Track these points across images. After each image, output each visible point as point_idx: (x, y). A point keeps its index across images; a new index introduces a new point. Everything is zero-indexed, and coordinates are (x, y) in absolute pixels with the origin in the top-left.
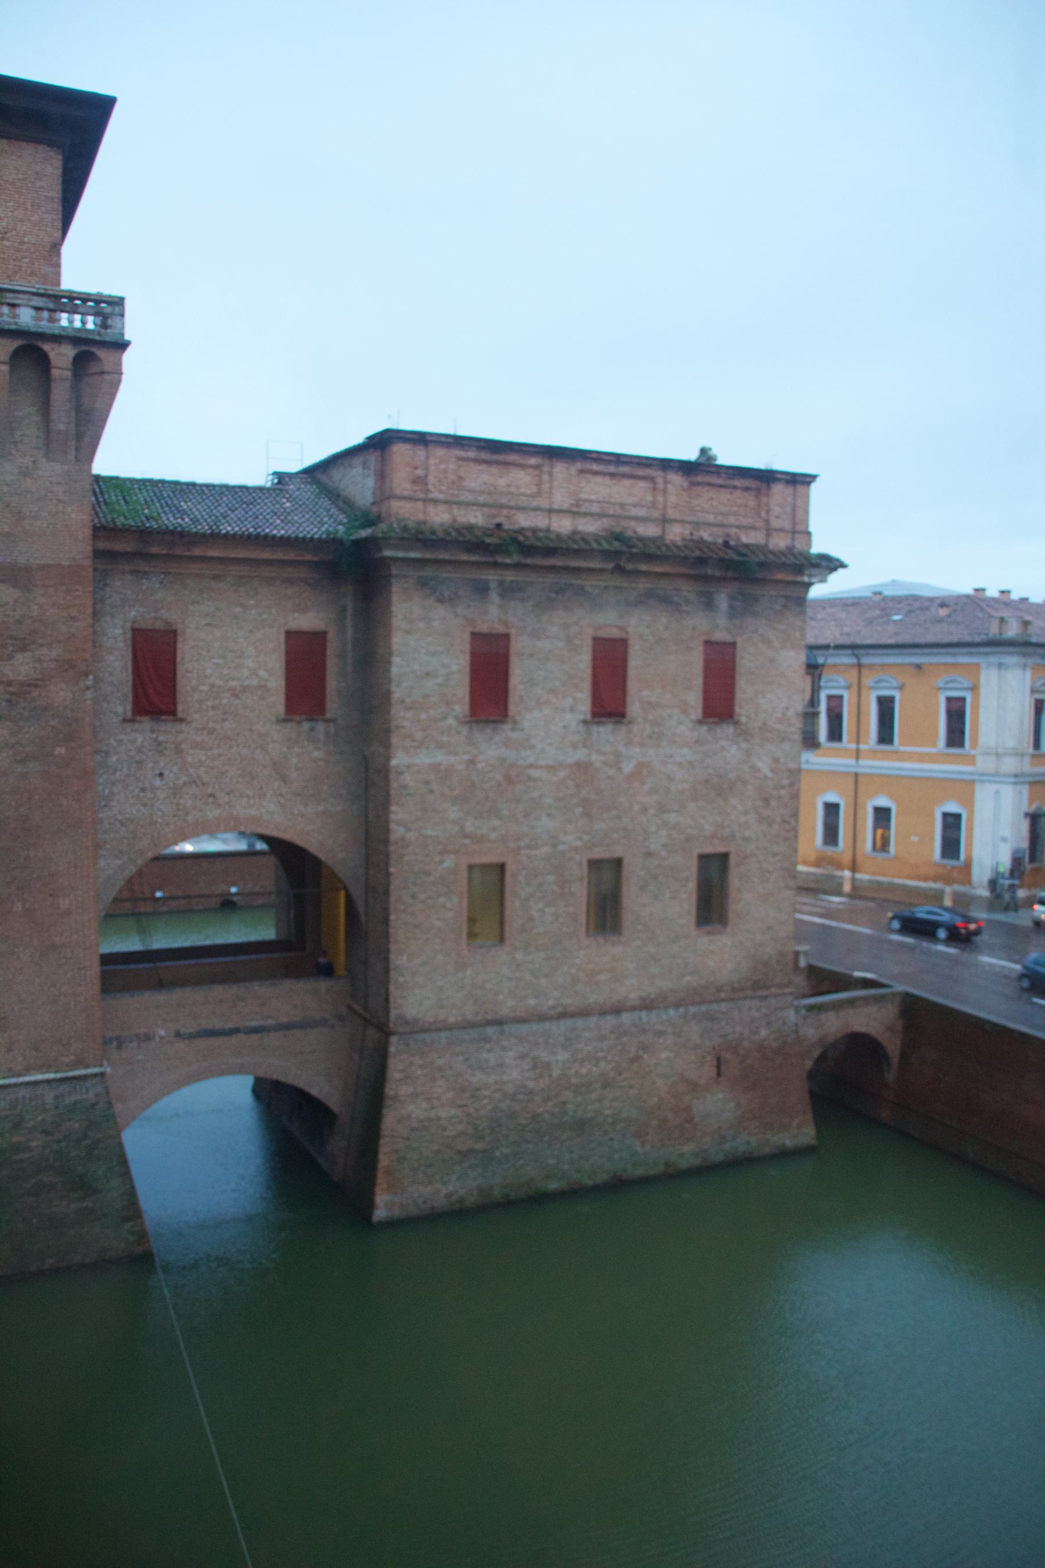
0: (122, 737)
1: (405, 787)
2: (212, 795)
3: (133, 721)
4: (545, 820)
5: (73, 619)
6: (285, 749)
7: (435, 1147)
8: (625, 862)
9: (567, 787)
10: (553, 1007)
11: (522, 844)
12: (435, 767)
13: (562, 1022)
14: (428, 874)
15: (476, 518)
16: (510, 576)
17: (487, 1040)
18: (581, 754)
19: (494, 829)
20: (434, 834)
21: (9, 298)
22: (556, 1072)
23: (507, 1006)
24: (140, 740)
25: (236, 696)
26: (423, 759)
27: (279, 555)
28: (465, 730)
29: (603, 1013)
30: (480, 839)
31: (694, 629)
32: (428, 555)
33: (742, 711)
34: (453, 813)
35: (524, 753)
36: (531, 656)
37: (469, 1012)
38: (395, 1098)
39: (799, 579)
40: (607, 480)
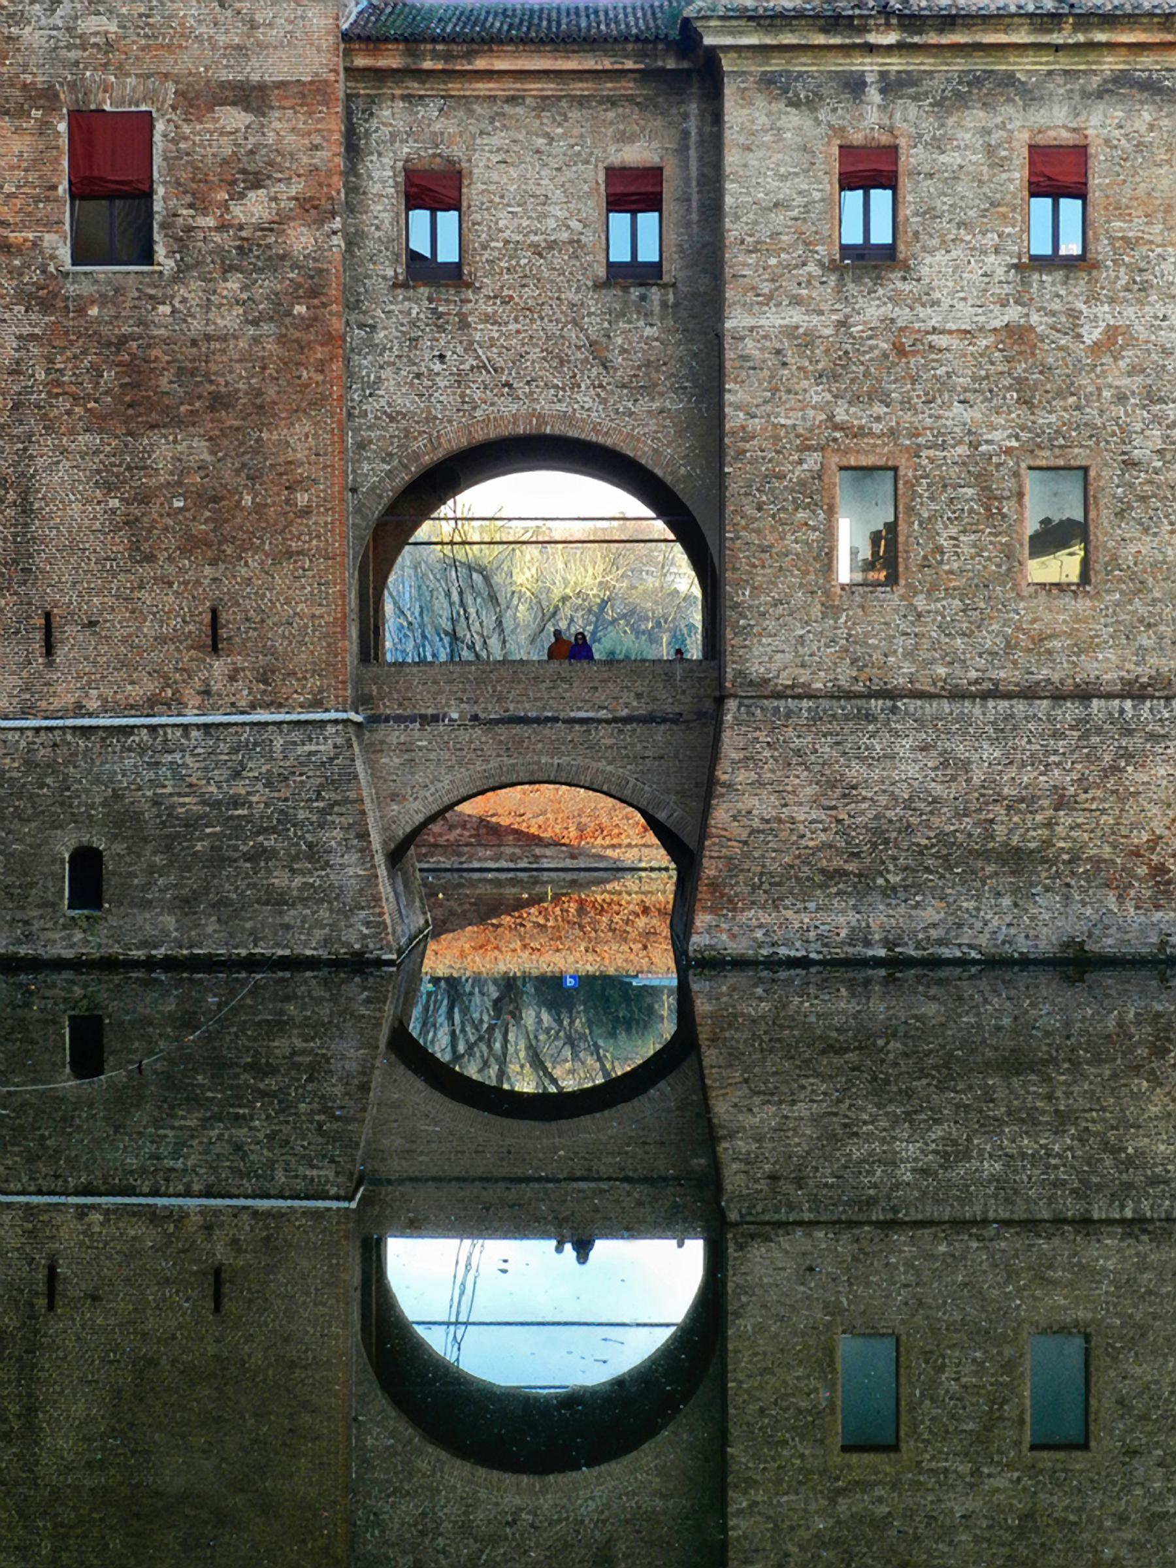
0: (392, 307)
1: (746, 358)
2: (507, 384)
3: (405, 285)
4: (957, 408)
5: (316, 147)
6: (606, 325)
8: (1092, 473)
9: (993, 363)
11: (920, 440)
12: (790, 332)
13: (991, 703)
14: (781, 477)
16: (895, 64)
17: (870, 718)
18: (1013, 314)
19: (878, 419)
20: (789, 422)
22: (978, 776)
23: (902, 673)
24: (414, 312)
25: (540, 255)
26: (774, 319)
27: (591, 63)
28: (833, 279)
29: (1058, 697)
30: (861, 433)
32: (769, 41)
34: (818, 395)
35: (923, 312)
36: (931, 176)
37: (845, 675)
38: (730, 786)
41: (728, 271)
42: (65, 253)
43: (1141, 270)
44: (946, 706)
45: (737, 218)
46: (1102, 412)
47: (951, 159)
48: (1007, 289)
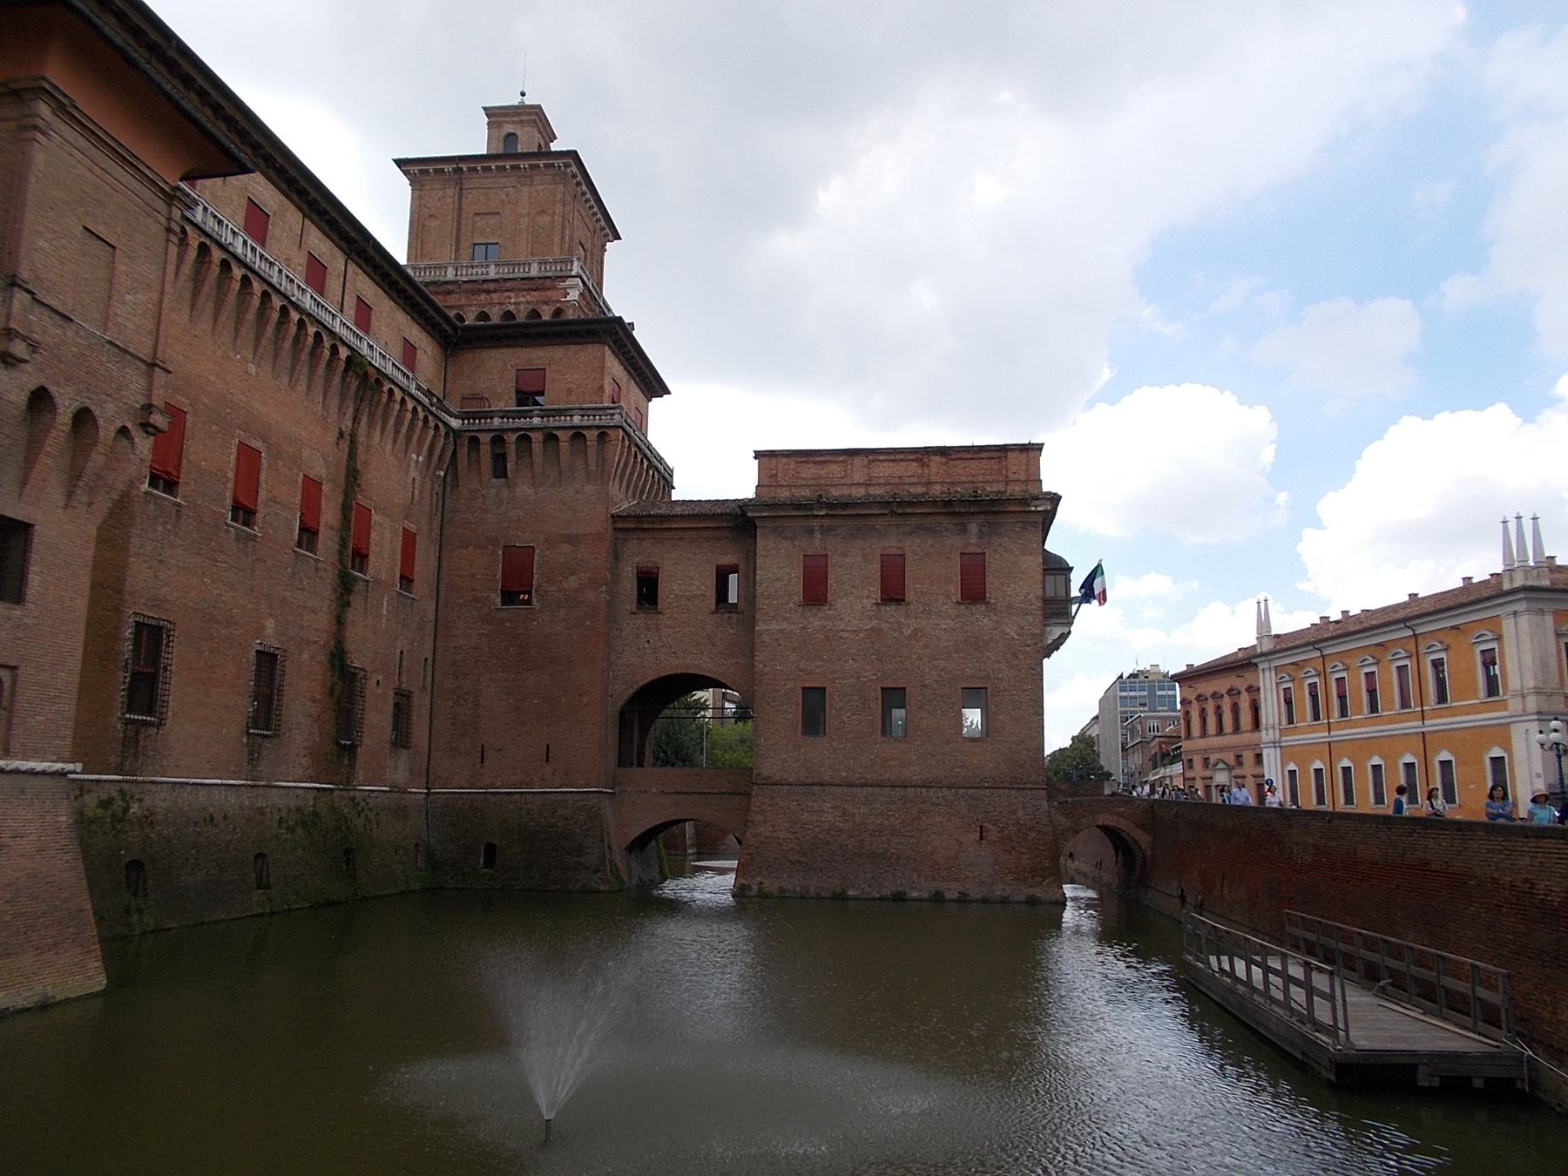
1: (763, 642)
3: (635, 613)
7: (775, 856)
10: (858, 779)
12: (781, 631)
14: (777, 691)
15: (807, 493)
16: (827, 522)
18: (874, 623)
21: (569, 413)
22: (858, 820)
26: (774, 626)
28: (800, 609)
31: (952, 546)
33: (991, 596)
39: (1027, 509)
40: (891, 464)
41: (757, 607)
42: (498, 601)
43: (928, 605)
44: (845, 789)
45: (761, 585)
46: (912, 664)
47: (849, 560)
48: (872, 613)
